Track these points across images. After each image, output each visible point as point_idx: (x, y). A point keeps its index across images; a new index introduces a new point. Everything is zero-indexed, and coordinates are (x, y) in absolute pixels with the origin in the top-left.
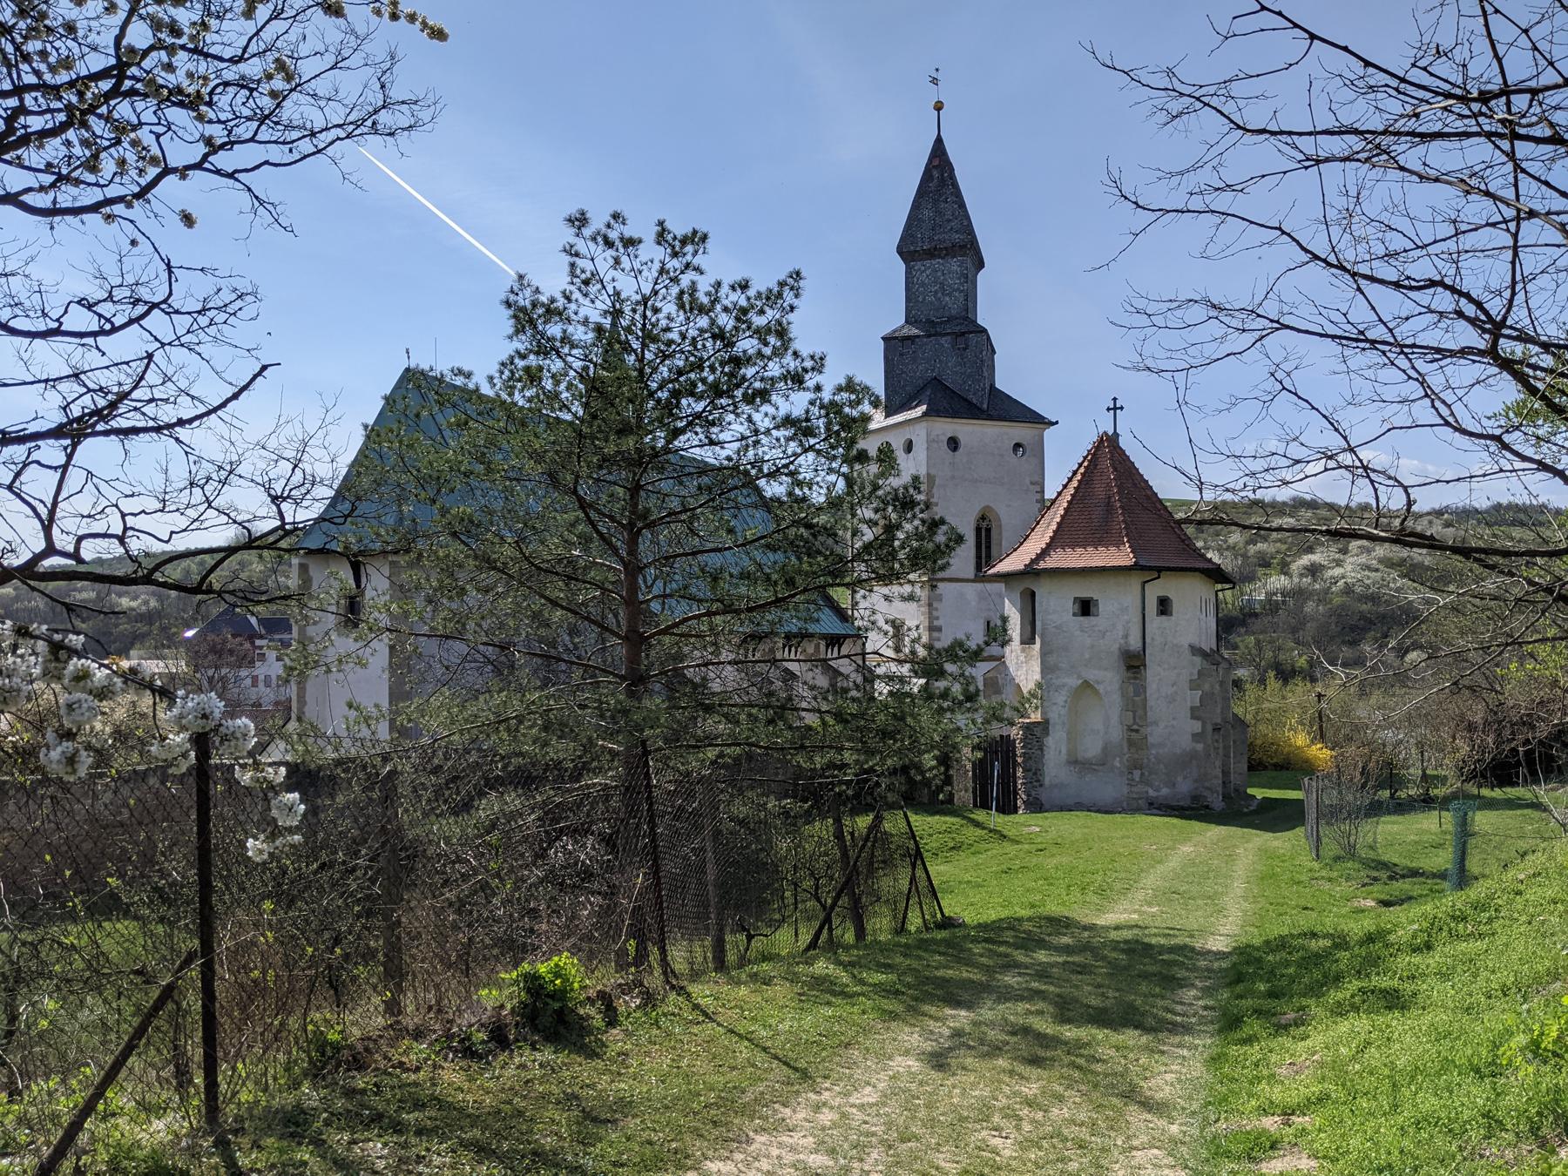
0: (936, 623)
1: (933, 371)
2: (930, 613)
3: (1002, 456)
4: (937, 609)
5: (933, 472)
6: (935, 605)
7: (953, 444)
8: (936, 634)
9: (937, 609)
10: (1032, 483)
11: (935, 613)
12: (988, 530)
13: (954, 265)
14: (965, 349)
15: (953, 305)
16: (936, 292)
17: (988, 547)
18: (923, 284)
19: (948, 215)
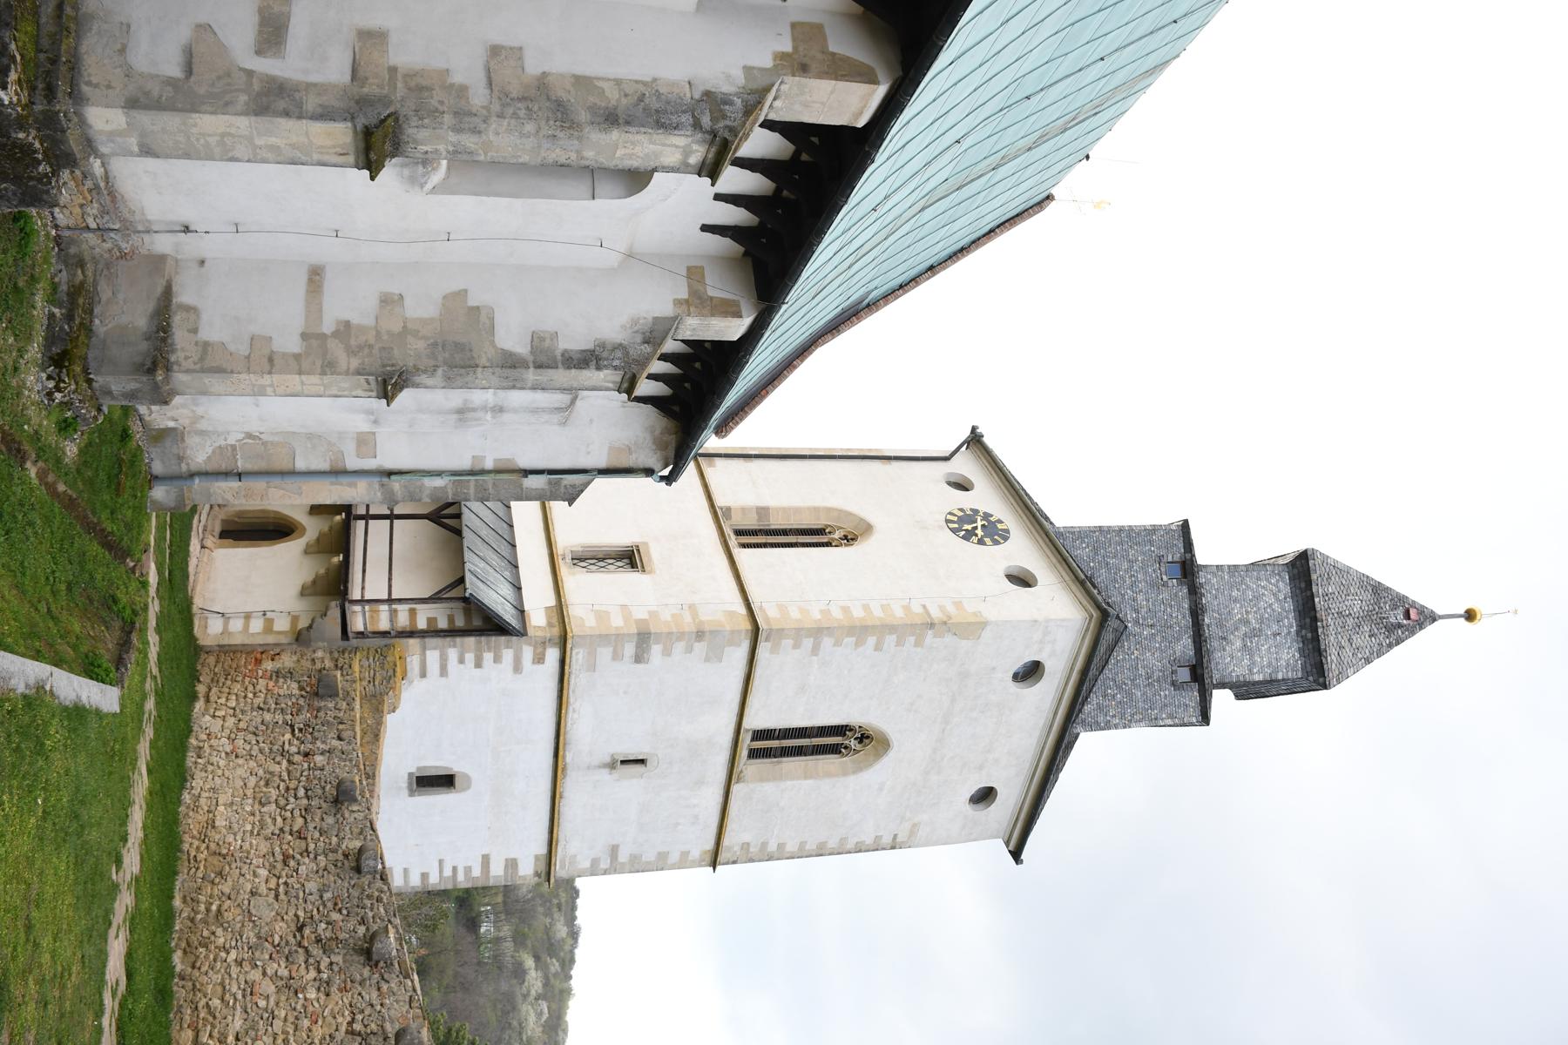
0: (656, 649)
1: (1136, 622)
2: (681, 636)
3: (981, 768)
4: (689, 650)
5: (987, 634)
6: (700, 647)
7: (1031, 672)
8: (629, 649)
9: (689, 650)
10: (915, 825)
11: (679, 647)
12: (834, 750)
13: (1285, 657)
14: (1173, 684)
15: (1229, 659)
16: (1247, 622)
17: (799, 751)
18: (1257, 598)
19: (1357, 640)
